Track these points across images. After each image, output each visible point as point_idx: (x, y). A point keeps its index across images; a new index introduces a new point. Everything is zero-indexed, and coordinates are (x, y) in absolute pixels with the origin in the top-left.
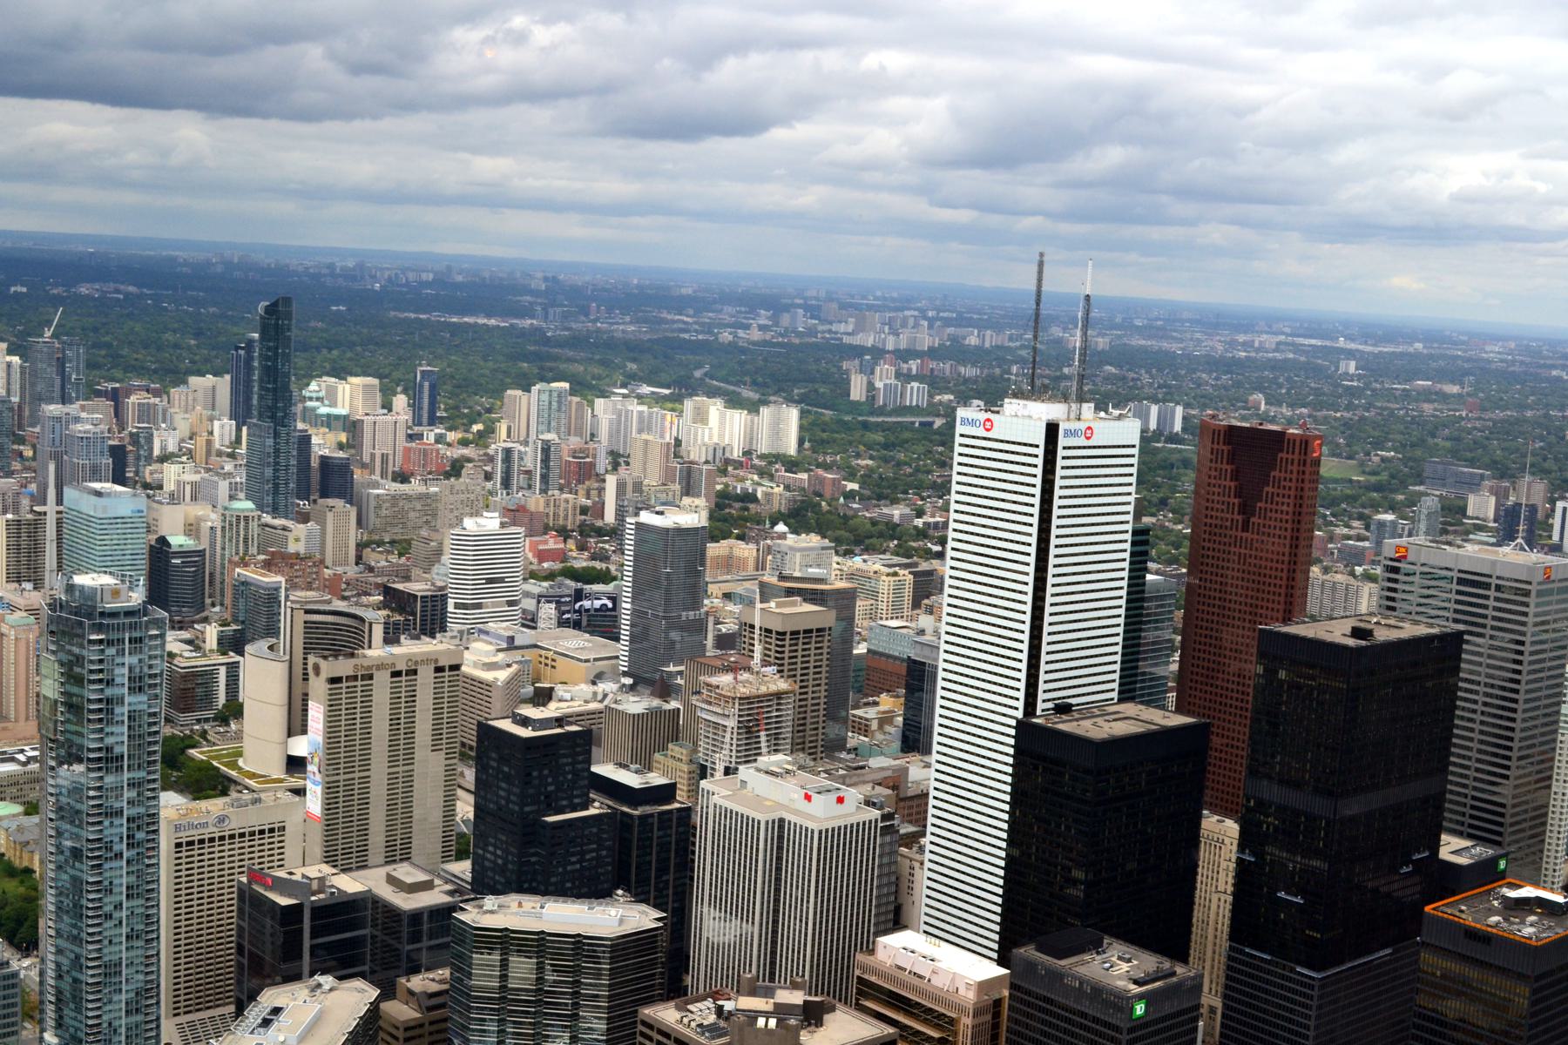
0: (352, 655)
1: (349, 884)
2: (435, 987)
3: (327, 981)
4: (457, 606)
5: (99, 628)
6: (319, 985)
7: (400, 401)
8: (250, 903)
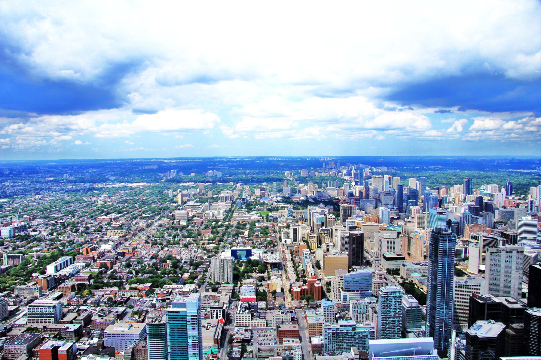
0: (496, 247)
1: (497, 300)
2: (519, 328)
3: (492, 321)
4: (520, 238)
5: (442, 237)
6: (490, 322)
7: (503, 190)
8: (473, 301)
